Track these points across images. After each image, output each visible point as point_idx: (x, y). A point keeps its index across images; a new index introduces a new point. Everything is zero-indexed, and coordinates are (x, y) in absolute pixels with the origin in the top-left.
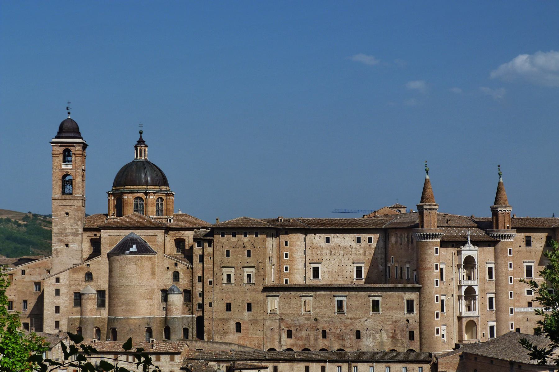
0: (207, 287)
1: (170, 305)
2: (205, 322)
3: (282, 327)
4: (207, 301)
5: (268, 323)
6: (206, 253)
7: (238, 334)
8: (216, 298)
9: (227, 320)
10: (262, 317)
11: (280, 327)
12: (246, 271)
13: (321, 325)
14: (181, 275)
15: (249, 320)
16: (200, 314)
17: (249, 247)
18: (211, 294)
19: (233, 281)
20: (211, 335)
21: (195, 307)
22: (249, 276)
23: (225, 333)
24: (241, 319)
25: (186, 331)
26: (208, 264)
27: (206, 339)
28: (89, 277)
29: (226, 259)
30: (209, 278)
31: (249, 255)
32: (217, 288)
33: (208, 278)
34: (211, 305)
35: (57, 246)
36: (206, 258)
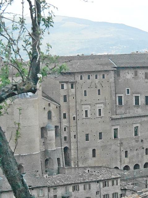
1: (50, 140)
2: (72, 151)
3: (122, 149)
4: (72, 134)
5: (113, 147)
6: (70, 94)
7: (94, 159)
10: (109, 143)
11: (120, 150)
14: (53, 114)
15: (102, 147)
16: (67, 145)
17: (99, 87)
18: (75, 128)
19: (89, 116)
20: (77, 162)
21: (63, 139)
22: (100, 110)
23: (86, 159)
24: (96, 146)
25: (58, 159)
26: (72, 103)
27: (73, 166)
29: (84, 98)
30: (73, 115)
31: (99, 94)
32: (79, 122)
33: (73, 114)
36: (71, 98)
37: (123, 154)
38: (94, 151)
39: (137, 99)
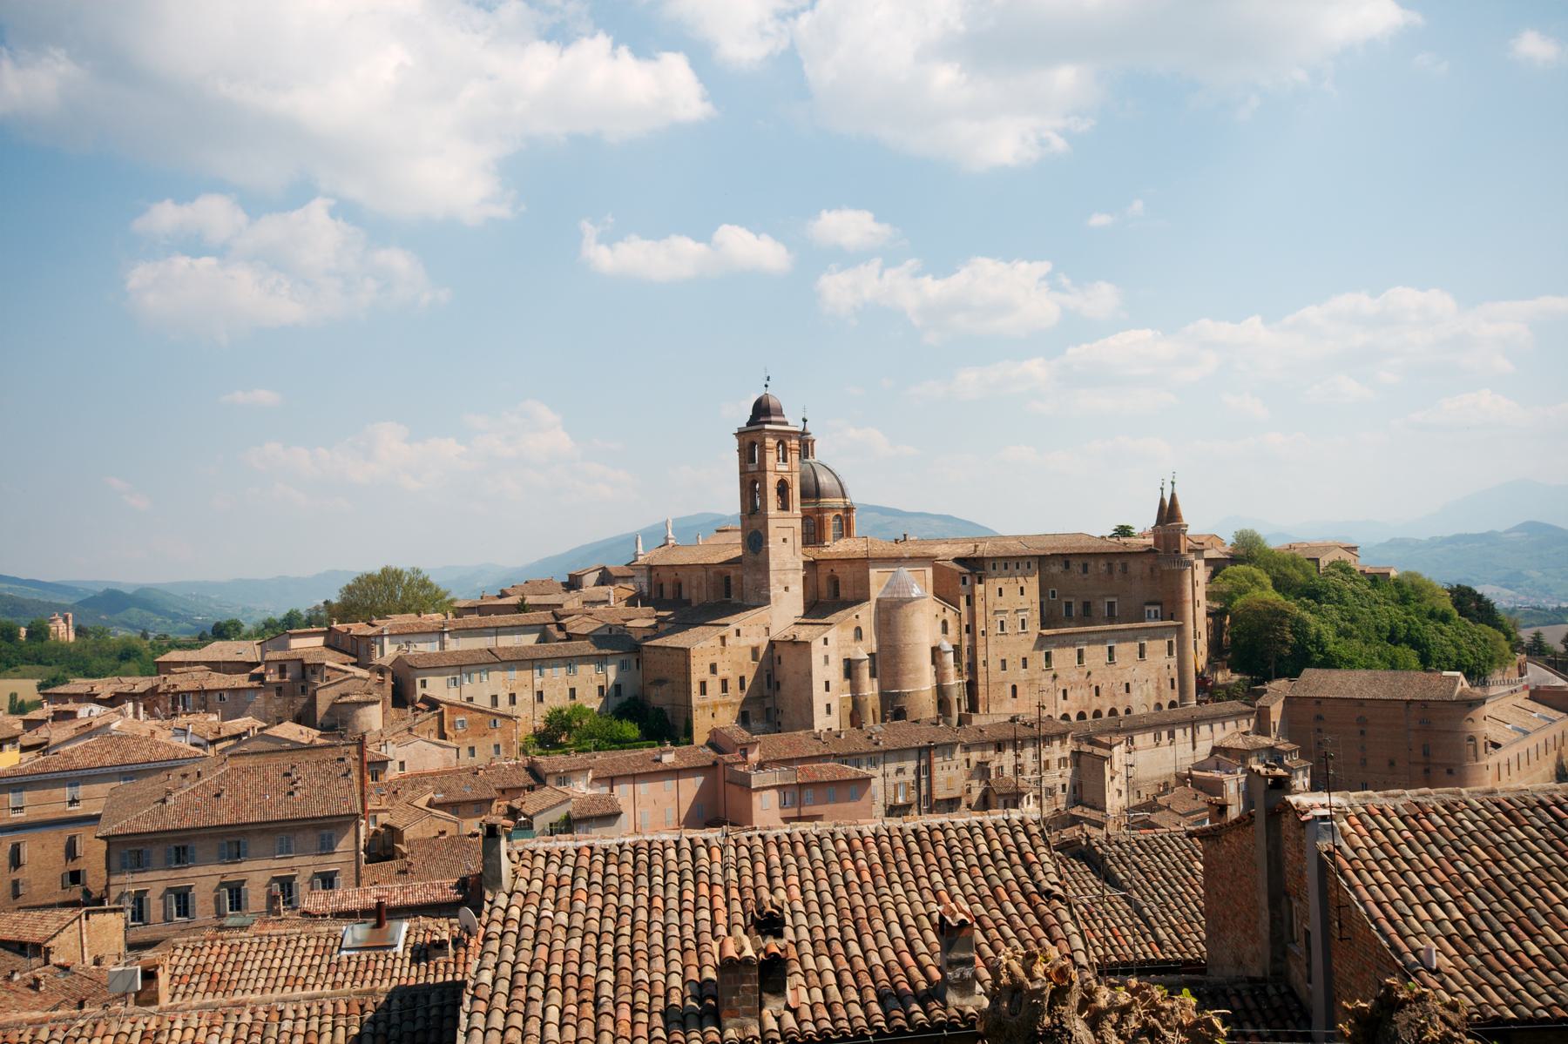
0: (980, 639)
4: (980, 659)
8: (991, 652)
9: (1002, 683)
12: (1021, 615)
13: (1094, 680)
14: (950, 626)
19: (1007, 630)
25: (959, 701)
26: (979, 609)
28: (859, 633)
32: (990, 640)
33: (980, 626)
34: (985, 663)
35: (775, 590)
36: (978, 600)
37: (1060, 695)
38: (1014, 688)
39: (1069, 605)
